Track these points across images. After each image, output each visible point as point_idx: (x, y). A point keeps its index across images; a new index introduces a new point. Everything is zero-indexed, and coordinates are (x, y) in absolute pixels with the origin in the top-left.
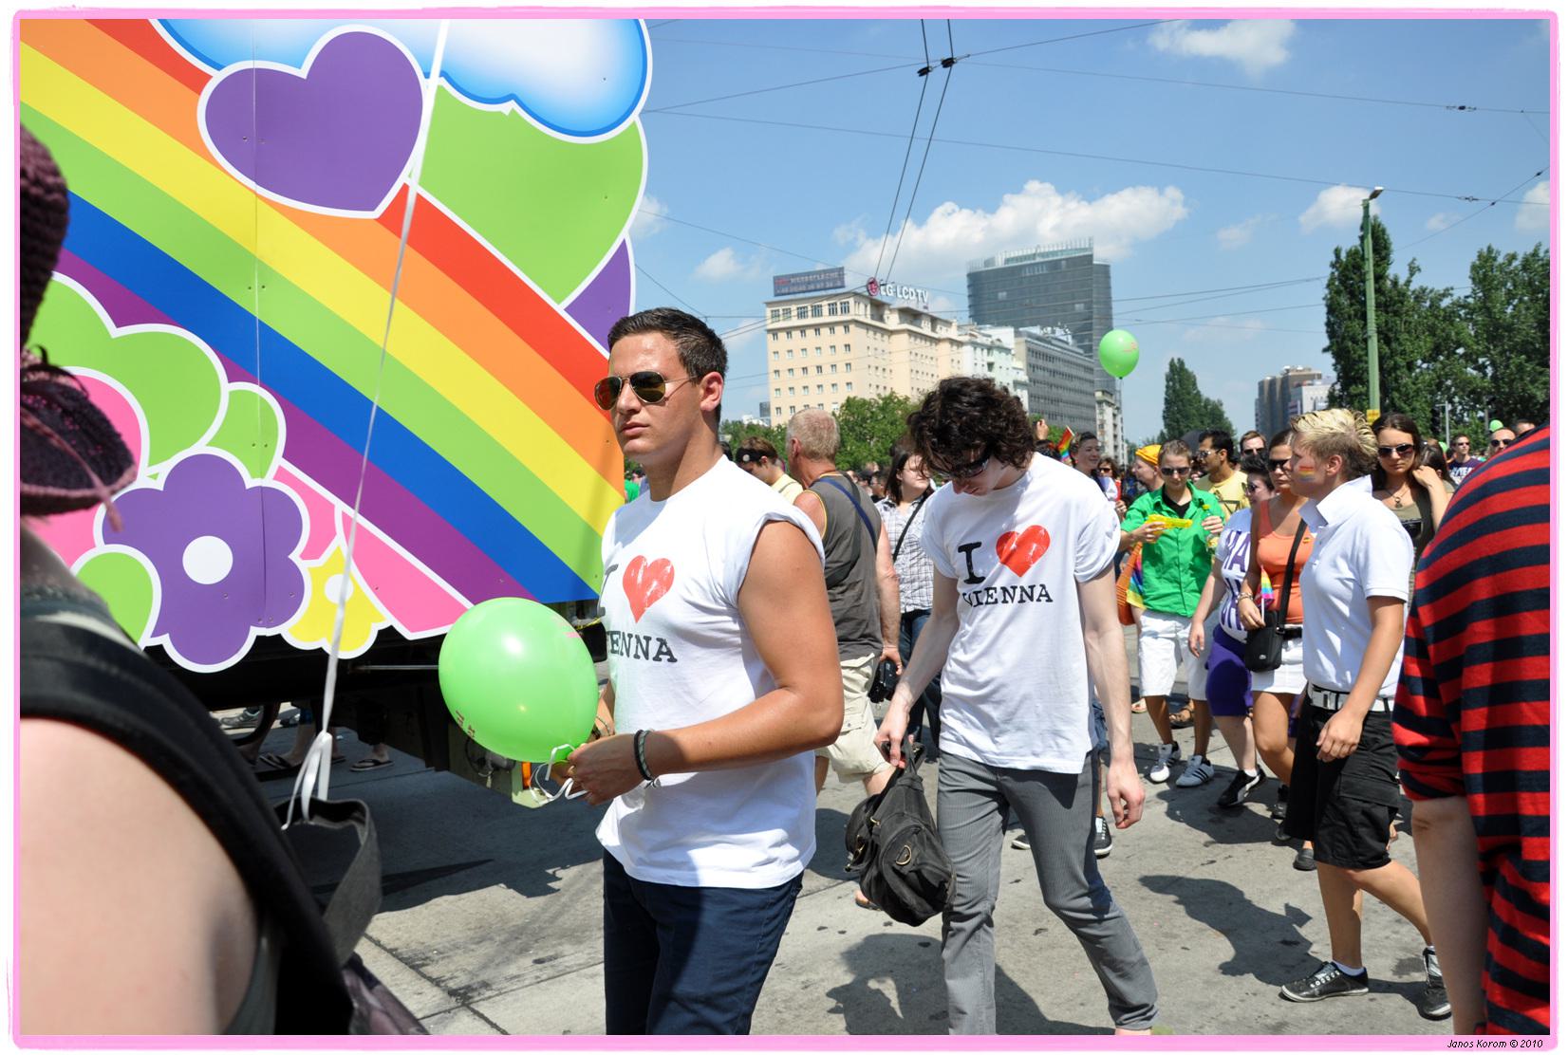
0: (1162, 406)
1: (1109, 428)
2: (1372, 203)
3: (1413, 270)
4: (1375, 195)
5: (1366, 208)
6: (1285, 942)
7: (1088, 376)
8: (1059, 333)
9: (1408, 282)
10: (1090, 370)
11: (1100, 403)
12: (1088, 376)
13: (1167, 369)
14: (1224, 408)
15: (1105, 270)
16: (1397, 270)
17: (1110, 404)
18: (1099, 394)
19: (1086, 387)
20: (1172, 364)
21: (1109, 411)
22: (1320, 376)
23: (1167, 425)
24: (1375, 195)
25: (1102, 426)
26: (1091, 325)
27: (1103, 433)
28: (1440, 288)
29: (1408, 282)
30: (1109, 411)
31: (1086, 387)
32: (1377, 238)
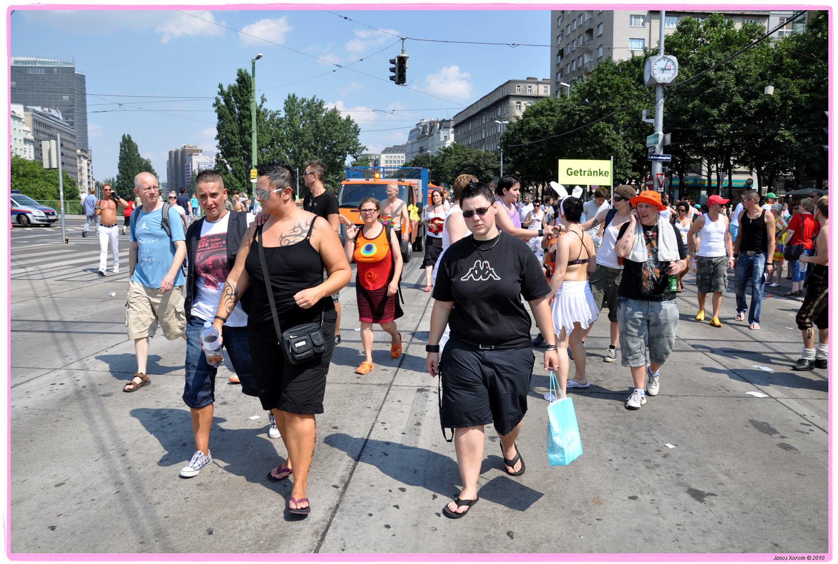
0: (118, 161)
1: (85, 171)
2: (257, 61)
3: (263, 100)
4: (258, 57)
5: (254, 64)
6: (631, 498)
7: (72, 140)
8: (54, 112)
9: (261, 106)
10: (73, 136)
11: (79, 156)
12: (72, 140)
13: (121, 140)
14: (152, 164)
15: (82, 78)
16: (257, 100)
17: (85, 158)
18: (79, 151)
19: (71, 146)
20: (124, 138)
21: (85, 162)
22: (201, 151)
23: (120, 172)
24: (258, 57)
25: (81, 170)
26: (76, 112)
27: (81, 174)
28: (275, 110)
29: (261, 106)
30: (85, 162)
31: (71, 146)
32: (244, 83)
